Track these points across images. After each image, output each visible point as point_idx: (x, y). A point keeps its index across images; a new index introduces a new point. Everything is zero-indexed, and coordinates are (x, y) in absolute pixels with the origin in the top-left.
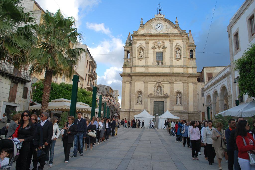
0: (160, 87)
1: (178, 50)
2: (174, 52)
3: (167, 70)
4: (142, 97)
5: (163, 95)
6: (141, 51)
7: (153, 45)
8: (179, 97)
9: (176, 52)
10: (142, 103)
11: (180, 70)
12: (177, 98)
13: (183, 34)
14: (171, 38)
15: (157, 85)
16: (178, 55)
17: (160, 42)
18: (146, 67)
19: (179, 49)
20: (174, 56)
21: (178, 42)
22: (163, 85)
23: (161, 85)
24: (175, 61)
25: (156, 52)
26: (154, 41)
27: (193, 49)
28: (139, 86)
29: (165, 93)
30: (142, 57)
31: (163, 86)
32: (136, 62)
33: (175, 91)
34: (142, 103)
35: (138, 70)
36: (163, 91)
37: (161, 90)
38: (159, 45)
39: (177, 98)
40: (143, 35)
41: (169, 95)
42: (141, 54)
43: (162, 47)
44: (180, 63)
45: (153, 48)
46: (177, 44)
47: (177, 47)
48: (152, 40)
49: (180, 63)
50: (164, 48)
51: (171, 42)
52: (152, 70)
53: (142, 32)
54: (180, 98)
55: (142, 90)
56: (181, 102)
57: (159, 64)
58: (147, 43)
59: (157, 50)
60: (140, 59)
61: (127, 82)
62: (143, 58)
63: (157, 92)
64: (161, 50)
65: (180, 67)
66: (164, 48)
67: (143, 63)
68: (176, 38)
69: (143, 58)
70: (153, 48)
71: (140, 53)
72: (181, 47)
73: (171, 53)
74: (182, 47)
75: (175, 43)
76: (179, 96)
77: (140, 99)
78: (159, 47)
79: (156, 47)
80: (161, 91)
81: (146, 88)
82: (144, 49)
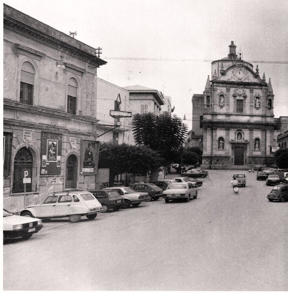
0: (241, 134)
1: (258, 99)
2: (254, 101)
4: (223, 144)
5: (243, 142)
7: (234, 93)
8: (258, 143)
9: (256, 101)
10: (223, 148)
12: (255, 144)
13: (263, 85)
14: (252, 87)
15: (238, 132)
16: (257, 104)
17: (241, 90)
18: (228, 115)
19: (258, 98)
20: (253, 104)
21: (258, 92)
22: (244, 132)
23: (241, 132)
24: (254, 110)
25: (237, 100)
28: (220, 133)
30: (223, 105)
31: (244, 133)
33: (254, 138)
34: (223, 148)
35: (221, 118)
37: (241, 136)
38: (240, 93)
39: (255, 144)
40: (224, 83)
41: (248, 141)
42: (222, 101)
45: (234, 96)
48: (233, 87)
50: (245, 97)
51: (251, 91)
52: (233, 119)
53: (223, 79)
54: (259, 144)
58: (228, 90)
59: (238, 98)
60: (222, 107)
61: (208, 129)
64: (242, 98)
65: (258, 116)
66: (245, 97)
67: (224, 110)
68: (256, 87)
74: (262, 96)
75: (255, 91)
76: (258, 142)
77: (221, 144)
79: (237, 95)
80: (241, 138)
81: (228, 135)
82: (225, 96)
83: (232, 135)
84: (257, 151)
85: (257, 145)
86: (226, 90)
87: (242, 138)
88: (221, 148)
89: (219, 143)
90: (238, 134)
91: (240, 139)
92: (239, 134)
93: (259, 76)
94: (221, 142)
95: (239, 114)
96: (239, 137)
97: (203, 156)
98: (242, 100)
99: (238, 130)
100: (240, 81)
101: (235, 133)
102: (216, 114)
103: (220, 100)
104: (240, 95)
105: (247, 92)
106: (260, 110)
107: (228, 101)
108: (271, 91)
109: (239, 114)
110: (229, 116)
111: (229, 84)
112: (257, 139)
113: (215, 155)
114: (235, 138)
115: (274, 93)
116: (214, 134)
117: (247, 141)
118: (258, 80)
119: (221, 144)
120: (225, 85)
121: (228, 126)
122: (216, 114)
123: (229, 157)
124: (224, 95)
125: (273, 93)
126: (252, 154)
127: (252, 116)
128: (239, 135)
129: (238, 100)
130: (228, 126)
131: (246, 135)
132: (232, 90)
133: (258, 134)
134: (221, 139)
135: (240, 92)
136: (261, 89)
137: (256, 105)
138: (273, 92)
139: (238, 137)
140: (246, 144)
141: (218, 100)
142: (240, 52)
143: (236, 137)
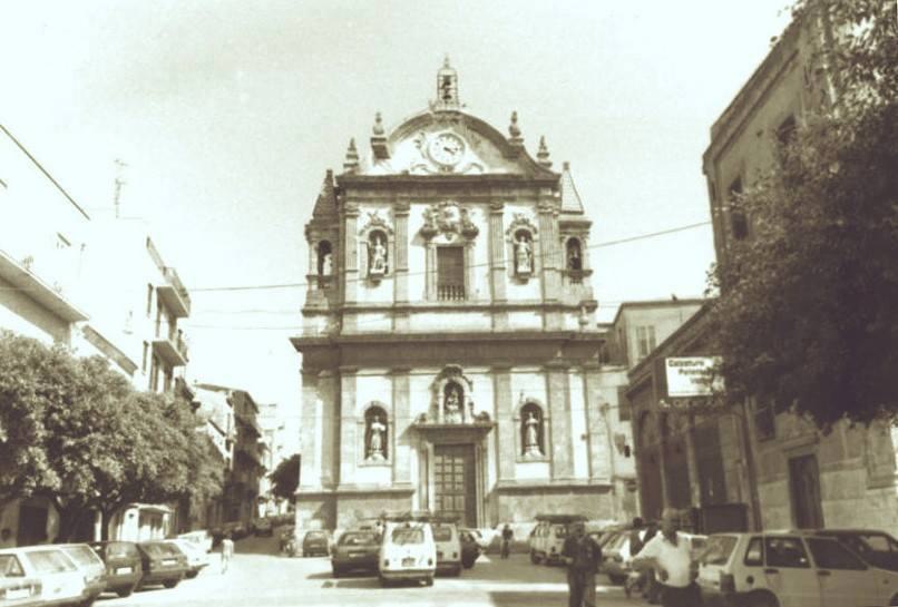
3: (478, 322)
4: (384, 434)
5: (470, 421)
8: (535, 425)
9: (516, 248)
11: (529, 321)
12: (524, 430)
13: (538, 182)
18: (399, 310)
19: (523, 235)
22: (469, 377)
26: (428, 206)
27: (578, 237)
28: (368, 388)
29: (477, 412)
30: (382, 271)
31: (470, 383)
32: (357, 292)
36: (471, 404)
38: (449, 221)
42: (378, 257)
44: (530, 292)
46: (520, 218)
47: (520, 227)
49: (530, 292)
50: (470, 234)
51: (495, 212)
54: (539, 428)
55: (385, 401)
56: (540, 442)
57: (449, 296)
58: (400, 213)
59: (441, 239)
60: (374, 280)
62: (386, 271)
63: (445, 408)
67: (383, 294)
69: (386, 271)
70: (426, 235)
72: (535, 231)
73: (493, 254)
75: (509, 211)
77: (376, 439)
78: (447, 229)
80: (461, 405)
83: (418, 395)
84: (535, 461)
85: (532, 433)
86: (393, 213)
87: (467, 407)
89: (369, 433)
92: (454, 391)
93: (523, 148)
94: (376, 426)
95: (450, 303)
97: (299, 491)
99: (446, 373)
100: (446, 173)
102: (356, 310)
104: (447, 229)
105: (477, 216)
106: (534, 283)
107: (401, 256)
109: (450, 303)
110: (406, 316)
111: (400, 189)
112: (530, 409)
113: (352, 485)
114: (436, 407)
116: (345, 396)
117: (485, 416)
118: (520, 164)
119: (376, 439)
120: (386, 194)
121: (396, 354)
122: (356, 310)
127: (498, 308)
128: (454, 392)
129: (441, 250)
130: (396, 354)
131: (480, 391)
132: (417, 214)
133: (528, 384)
134: (375, 413)
135: (448, 215)
140: (484, 427)
141: (362, 251)
143: (441, 402)
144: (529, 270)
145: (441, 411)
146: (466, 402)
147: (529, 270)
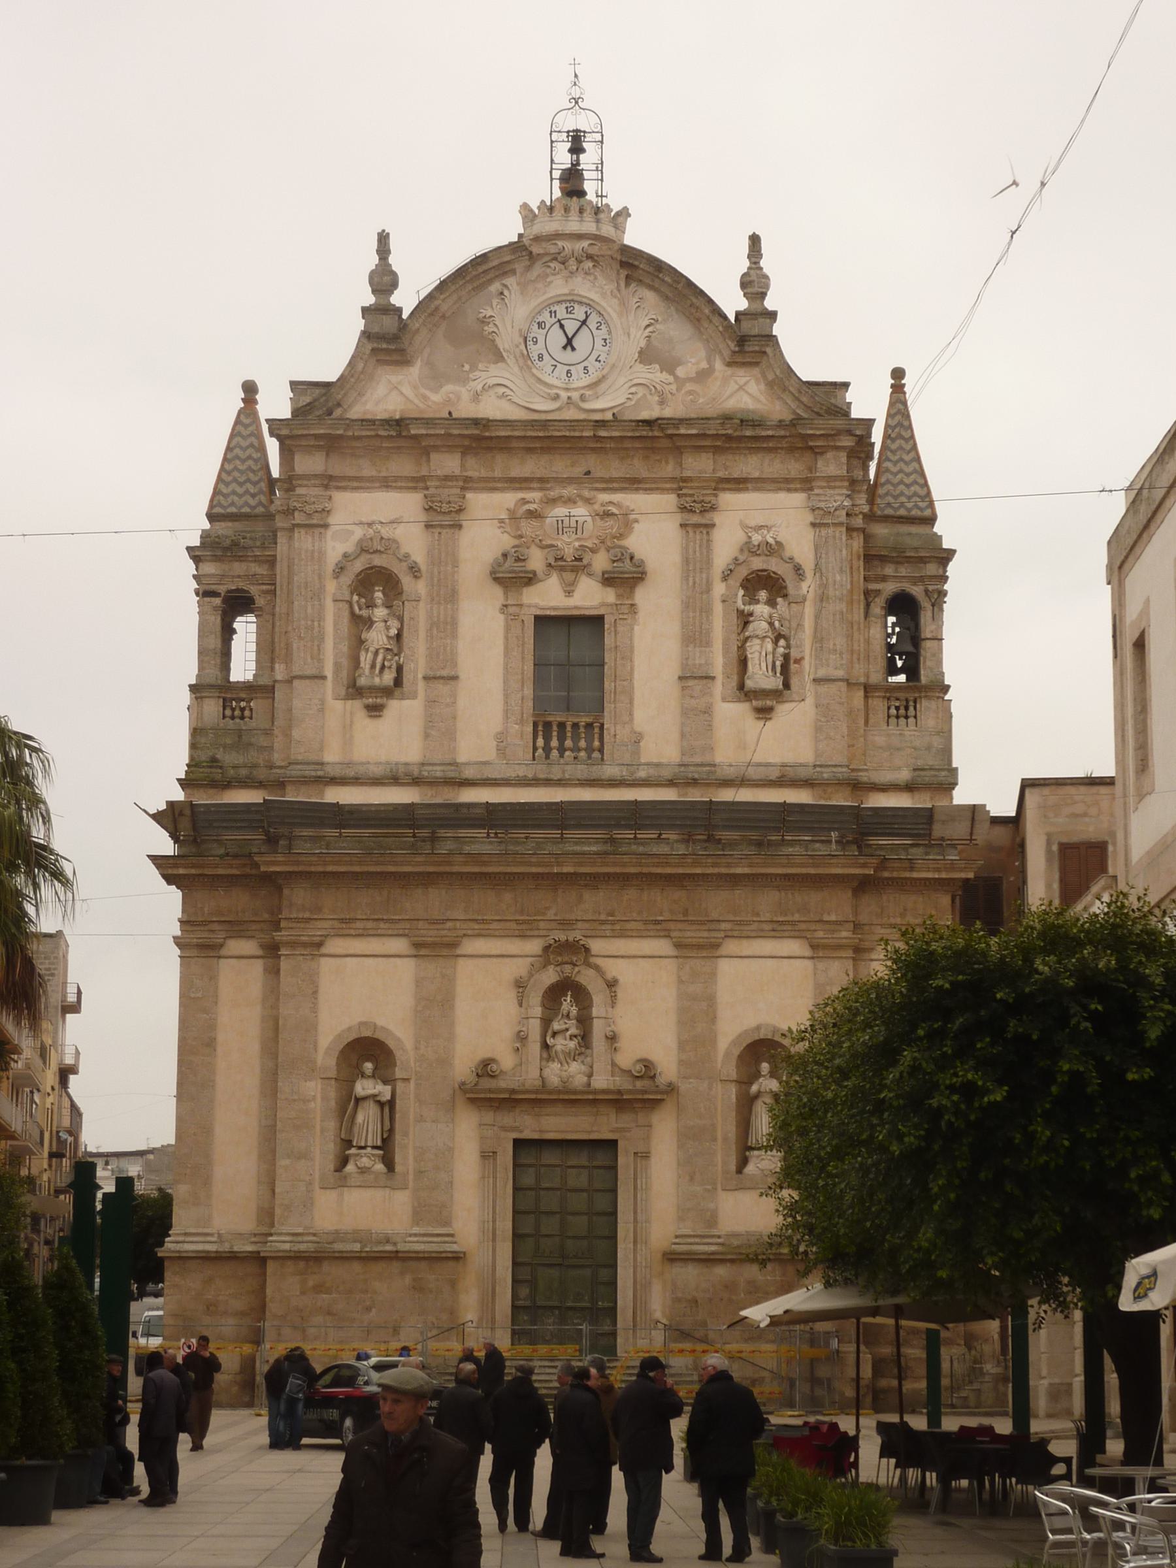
0: (581, 995)
1: (763, 595)
2: (719, 625)
4: (388, 1107)
5: (601, 1081)
6: (380, 613)
9: (745, 619)
10: (389, 1164)
14: (699, 465)
15: (550, 976)
20: (718, 661)
22: (614, 969)
23: (586, 977)
25: (538, 619)
27: (917, 591)
29: (626, 1059)
30: (388, 678)
31: (612, 984)
34: (389, 1164)
36: (612, 1038)
37: (585, 1020)
38: (568, 545)
42: (377, 637)
43: (600, 562)
47: (757, 563)
48: (490, 485)
57: (562, 750)
61: (237, 946)
63: (546, 1046)
68: (749, 465)
69: (398, 682)
71: (369, 623)
72: (798, 570)
74: (808, 565)
77: (367, 1119)
79: (536, 560)
80: (585, 1038)
82: (406, 581)
88: (370, 1160)
89: (348, 1104)
90: (554, 994)
91: (573, 1056)
93: (772, 339)
94: (364, 1087)
96: (556, 1026)
97: (171, 1245)
98: (598, 620)
101: (520, 985)
103: (361, 623)
108: (911, 507)
114: (521, 1038)
115: (947, 530)
119: (367, 1119)
123: (458, 1258)
124: (400, 570)
125: (938, 528)
126: (712, 1220)
128: (568, 1004)
136: (806, 484)
137: (743, 662)
138: (931, 520)
139: (546, 1022)
142: (571, 122)
143: (535, 1027)
144: (776, 682)
145: (535, 1048)
146: (598, 1029)
147: (776, 682)
